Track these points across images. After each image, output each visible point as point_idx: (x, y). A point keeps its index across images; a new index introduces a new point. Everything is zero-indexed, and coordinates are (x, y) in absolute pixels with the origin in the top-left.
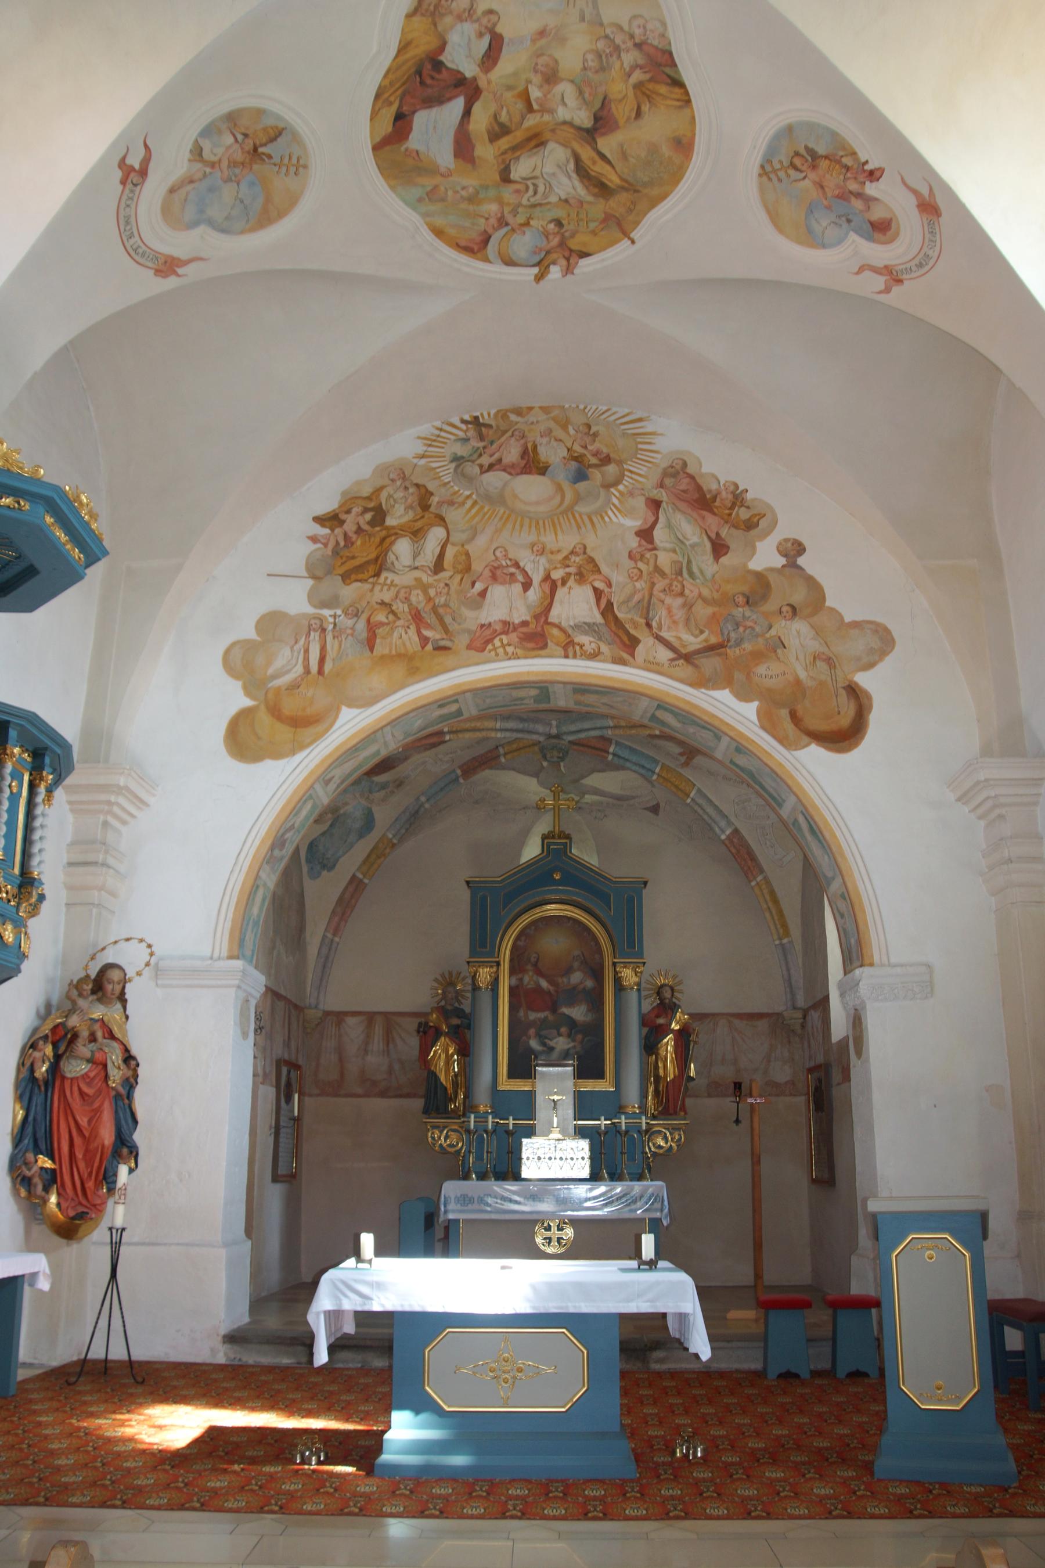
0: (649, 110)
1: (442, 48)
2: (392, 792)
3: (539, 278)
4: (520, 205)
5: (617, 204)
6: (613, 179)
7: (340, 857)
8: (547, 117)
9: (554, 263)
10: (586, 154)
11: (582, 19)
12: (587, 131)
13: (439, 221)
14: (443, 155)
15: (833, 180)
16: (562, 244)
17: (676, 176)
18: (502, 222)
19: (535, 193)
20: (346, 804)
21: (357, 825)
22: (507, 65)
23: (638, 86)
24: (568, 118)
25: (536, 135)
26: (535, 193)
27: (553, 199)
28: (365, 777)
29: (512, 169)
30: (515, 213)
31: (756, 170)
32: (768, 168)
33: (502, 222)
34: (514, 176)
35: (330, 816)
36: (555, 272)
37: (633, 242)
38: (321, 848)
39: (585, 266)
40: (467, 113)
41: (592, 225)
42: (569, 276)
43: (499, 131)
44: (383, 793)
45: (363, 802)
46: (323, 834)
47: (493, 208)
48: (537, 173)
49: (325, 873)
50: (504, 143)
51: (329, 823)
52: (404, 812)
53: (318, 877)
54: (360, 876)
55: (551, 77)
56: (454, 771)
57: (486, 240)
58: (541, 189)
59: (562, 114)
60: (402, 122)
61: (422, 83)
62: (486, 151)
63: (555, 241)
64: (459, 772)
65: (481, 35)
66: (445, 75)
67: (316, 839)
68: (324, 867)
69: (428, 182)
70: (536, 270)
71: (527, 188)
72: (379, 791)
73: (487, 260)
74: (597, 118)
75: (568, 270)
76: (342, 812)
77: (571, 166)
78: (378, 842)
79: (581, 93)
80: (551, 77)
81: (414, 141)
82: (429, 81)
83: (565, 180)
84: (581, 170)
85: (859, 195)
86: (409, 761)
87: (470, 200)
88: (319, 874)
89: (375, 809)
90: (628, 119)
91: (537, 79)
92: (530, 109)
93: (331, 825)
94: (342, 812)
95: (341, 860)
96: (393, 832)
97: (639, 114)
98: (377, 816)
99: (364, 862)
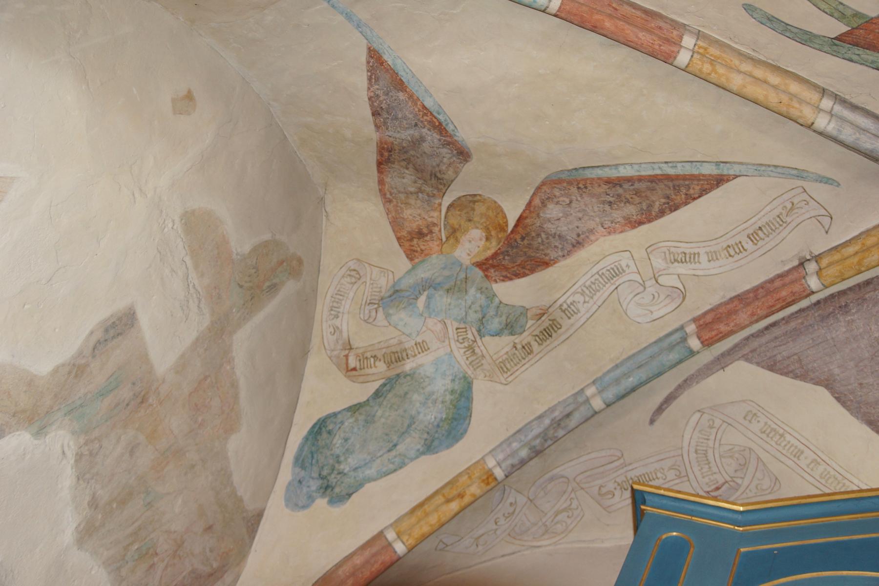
2: (527, 349)
7: (370, 480)
20: (422, 347)
21: (431, 415)
28: (479, 273)
35: (381, 367)
38: (338, 441)
44: (506, 341)
45: (459, 354)
46: (355, 409)
49: (321, 503)
51: (376, 385)
52: (540, 417)
53: (304, 507)
54: (391, 535)
56: (682, 328)
64: (691, 328)
67: (335, 415)
68: (326, 488)
72: (498, 334)
76: (409, 366)
78: (460, 475)
86: (582, 254)
88: (311, 499)
89: (480, 387)
93: (377, 394)
94: (409, 366)
95: (368, 486)
96: (501, 456)
98: (481, 406)
99: (413, 510)
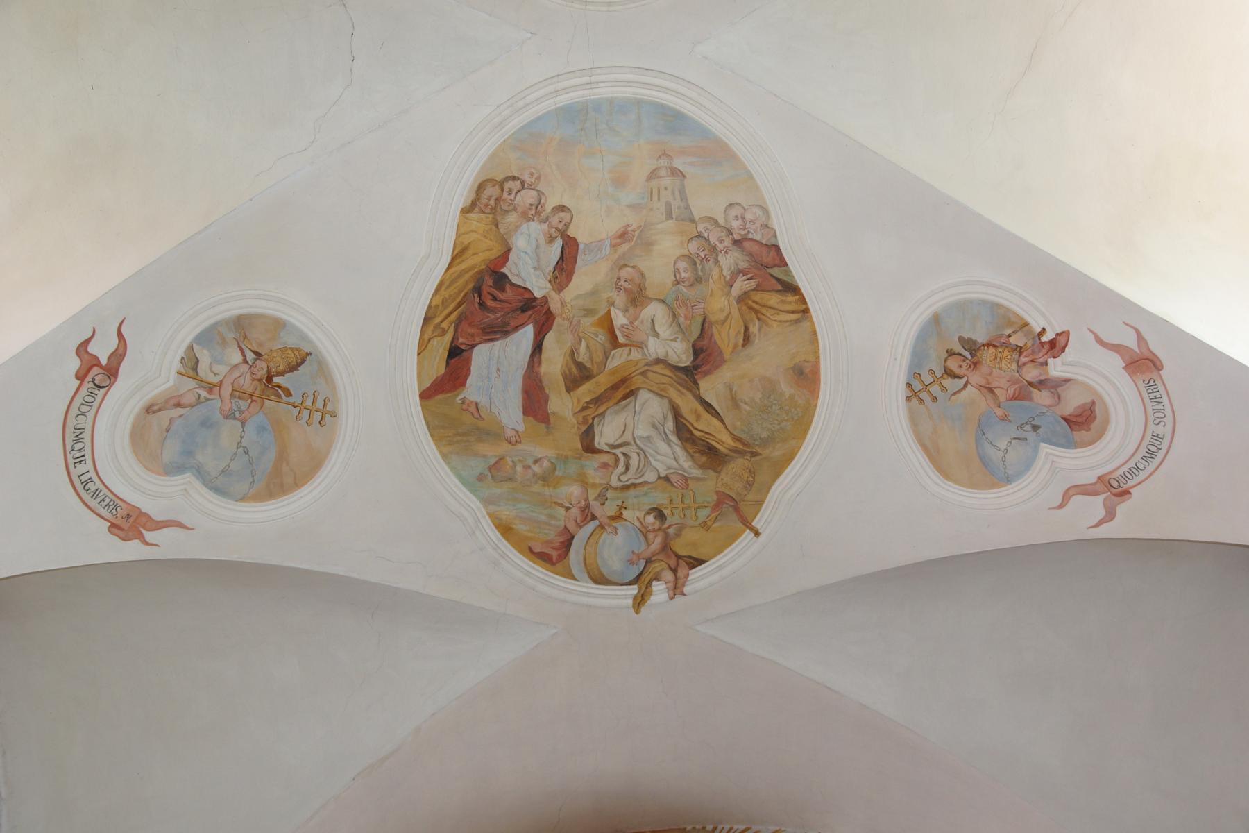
0: (759, 330)
1: (505, 257)
3: (639, 602)
4: (608, 487)
5: (731, 477)
6: (723, 441)
8: (636, 355)
9: (657, 578)
10: (687, 405)
11: (669, 216)
12: (685, 370)
13: (506, 512)
14: (510, 413)
15: (1003, 372)
16: (666, 547)
17: (802, 423)
18: (587, 515)
19: (627, 469)
22: (584, 280)
23: (743, 298)
24: (661, 354)
25: (623, 381)
26: (627, 469)
27: (650, 477)
29: (597, 430)
30: (601, 497)
31: (902, 392)
32: (917, 386)
33: (587, 515)
34: (600, 442)
36: (659, 590)
37: (757, 534)
39: (698, 579)
40: (538, 348)
41: (703, 514)
42: (679, 598)
43: (578, 375)
47: (573, 491)
48: (627, 437)
50: (586, 391)
55: (637, 297)
57: (567, 544)
58: (634, 462)
59: (655, 348)
60: (457, 354)
61: (482, 304)
62: (562, 404)
63: (657, 542)
65: (551, 239)
66: (509, 294)
69: (491, 451)
70: (633, 590)
71: (617, 460)
73: (570, 575)
74: (697, 351)
75: (676, 589)
77: (670, 425)
79: (675, 316)
80: (637, 297)
81: (473, 390)
82: (490, 303)
83: (663, 446)
84: (683, 431)
85: (1041, 384)
87: (545, 479)
90: (735, 346)
91: (620, 299)
92: (615, 343)
97: (747, 339)
